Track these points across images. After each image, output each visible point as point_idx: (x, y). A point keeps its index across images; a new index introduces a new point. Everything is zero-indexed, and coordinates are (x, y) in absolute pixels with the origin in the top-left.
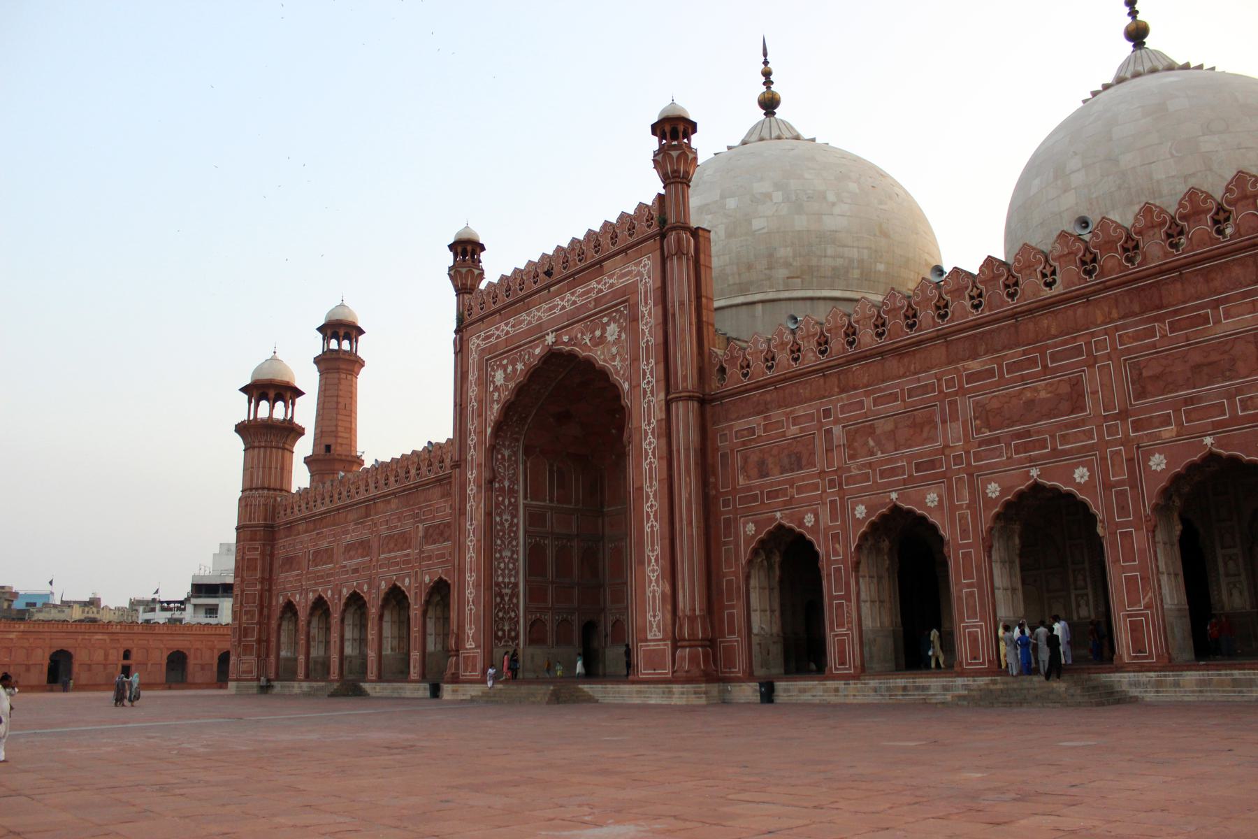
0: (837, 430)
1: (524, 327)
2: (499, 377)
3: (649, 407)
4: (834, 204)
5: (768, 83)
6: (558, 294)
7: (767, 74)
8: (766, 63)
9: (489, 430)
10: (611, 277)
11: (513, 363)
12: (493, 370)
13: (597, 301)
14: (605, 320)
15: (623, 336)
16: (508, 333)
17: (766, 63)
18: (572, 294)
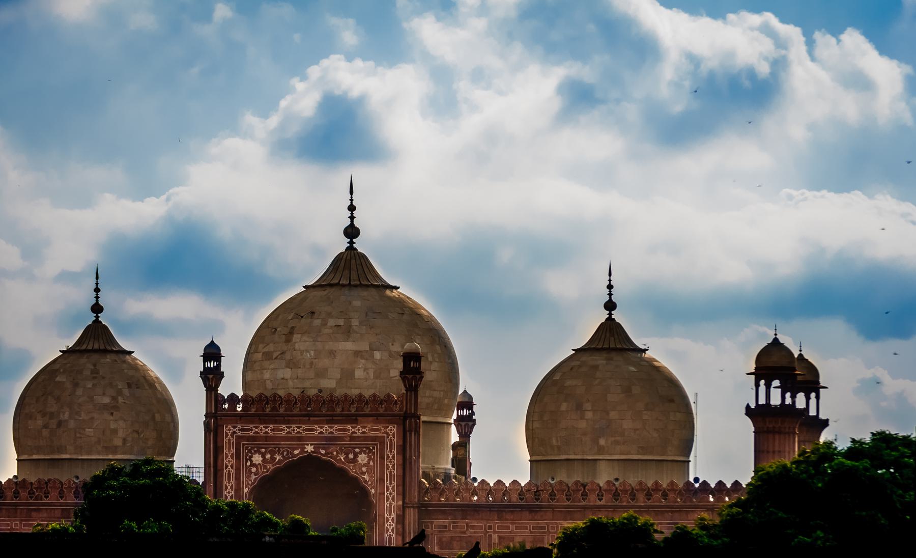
0: (495, 537)
1: (283, 434)
2: (257, 459)
3: (390, 506)
4: (431, 362)
5: (352, 218)
6: (316, 422)
7: (352, 208)
8: (352, 200)
9: (246, 490)
10: (364, 427)
11: (273, 454)
12: (250, 451)
13: (352, 438)
14: (357, 450)
15: (372, 463)
16: (266, 433)
17: (352, 200)
18: (331, 427)
